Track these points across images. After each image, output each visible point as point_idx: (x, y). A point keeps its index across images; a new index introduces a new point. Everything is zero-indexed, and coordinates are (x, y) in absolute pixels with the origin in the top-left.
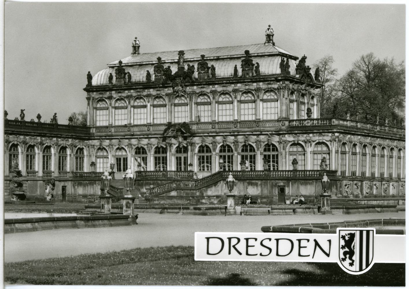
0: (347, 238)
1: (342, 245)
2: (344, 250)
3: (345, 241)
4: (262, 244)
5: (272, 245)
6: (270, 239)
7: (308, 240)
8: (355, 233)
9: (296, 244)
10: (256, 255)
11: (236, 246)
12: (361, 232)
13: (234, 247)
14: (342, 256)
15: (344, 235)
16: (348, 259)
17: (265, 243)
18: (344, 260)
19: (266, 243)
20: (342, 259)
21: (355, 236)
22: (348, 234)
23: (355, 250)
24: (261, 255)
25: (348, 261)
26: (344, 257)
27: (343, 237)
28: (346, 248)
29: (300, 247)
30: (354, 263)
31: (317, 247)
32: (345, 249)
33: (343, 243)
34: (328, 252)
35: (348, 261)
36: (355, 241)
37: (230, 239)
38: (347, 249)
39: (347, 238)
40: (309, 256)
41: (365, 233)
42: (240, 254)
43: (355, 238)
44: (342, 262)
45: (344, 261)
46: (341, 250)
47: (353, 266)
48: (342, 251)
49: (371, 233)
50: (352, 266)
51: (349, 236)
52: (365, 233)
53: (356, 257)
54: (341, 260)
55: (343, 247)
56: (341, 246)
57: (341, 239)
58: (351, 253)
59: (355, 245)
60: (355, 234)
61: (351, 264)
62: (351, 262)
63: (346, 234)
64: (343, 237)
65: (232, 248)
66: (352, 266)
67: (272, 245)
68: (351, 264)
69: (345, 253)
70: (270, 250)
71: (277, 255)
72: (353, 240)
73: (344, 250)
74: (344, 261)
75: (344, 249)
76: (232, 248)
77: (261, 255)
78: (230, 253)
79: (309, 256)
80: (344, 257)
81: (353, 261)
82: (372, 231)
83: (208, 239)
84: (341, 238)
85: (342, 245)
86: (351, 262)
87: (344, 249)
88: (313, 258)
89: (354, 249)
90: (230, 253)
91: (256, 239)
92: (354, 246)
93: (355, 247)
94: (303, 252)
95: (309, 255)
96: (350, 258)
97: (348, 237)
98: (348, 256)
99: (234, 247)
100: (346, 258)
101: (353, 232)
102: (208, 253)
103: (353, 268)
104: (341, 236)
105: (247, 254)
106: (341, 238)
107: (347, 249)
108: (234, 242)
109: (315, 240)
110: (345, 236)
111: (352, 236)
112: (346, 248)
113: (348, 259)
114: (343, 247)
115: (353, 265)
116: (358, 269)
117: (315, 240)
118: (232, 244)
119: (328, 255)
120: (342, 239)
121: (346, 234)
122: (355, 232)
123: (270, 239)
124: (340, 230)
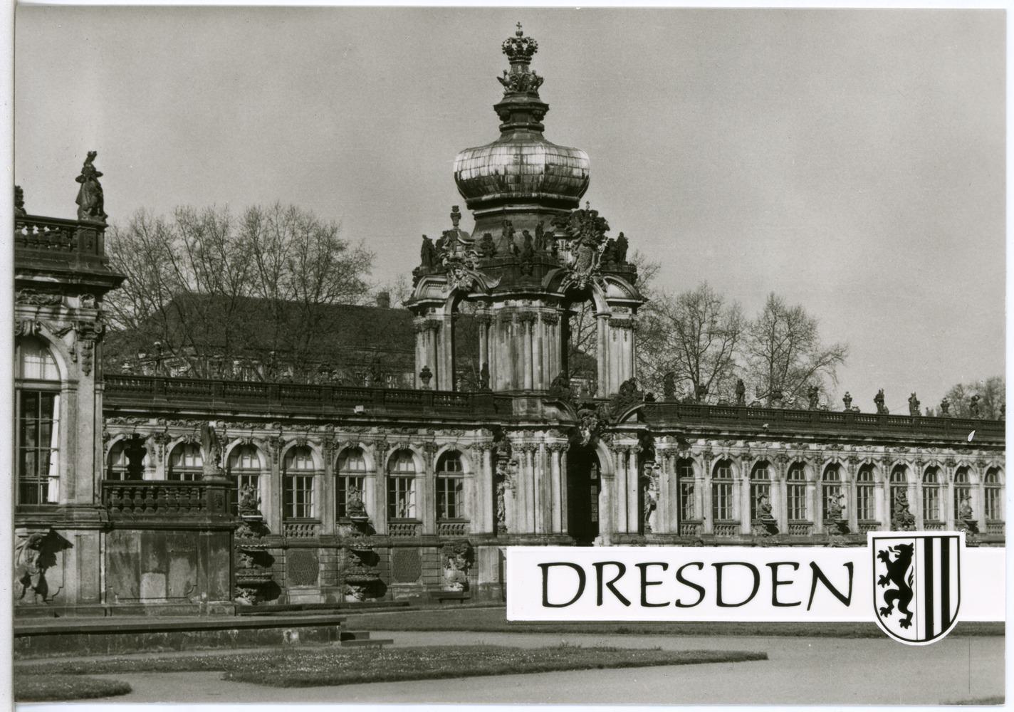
0: (893, 558)
1: (881, 576)
2: (887, 588)
3: (889, 565)
8: (912, 544)
12: (928, 542)
14: (882, 603)
15: (885, 549)
16: (896, 611)
18: (886, 612)
20: (882, 609)
21: (914, 552)
22: (896, 548)
23: (913, 588)
25: (897, 615)
26: (886, 606)
27: (884, 556)
28: (891, 581)
30: (913, 620)
32: (889, 584)
33: (882, 569)
35: (897, 615)
36: (913, 563)
38: (893, 586)
39: (893, 558)
41: (937, 545)
43: (913, 558)
44: (883, 618)
45: (886, 616)
46: (879, 587)
47: (909, 627)
48: (881, 591)
49: (953, 542)
50: (906, 628)
51: (898, 552)
52: (937, 545)
53: (917, 605)
54: (879, 612)
55: (884, 581)
56: (878, 579)
57: (879, 561)
58: (905, 595)
59: (914, 574)
60: (914, 547)
61: (905, 623)
62: (904, 616)
63: (890, 548)
64: (884, 556)
66: (906, 628)
68: (905, 623)
69: (889, 596)
72: (909, 562)
73: (887, 588)
74: (886, 616)
75: (886, 585)
80: (886, 606)
81: (910, 615)
82: (956, 539)
84: (879, 557)
85: (881, 576)
86: (904, 616)
87: (886, 585)
89: (911, 585)
92: (910, 577)
93: (914, 579)
96: (903, 608)
97: (896, 556)
98: (896, 602)
100: (891, 607)
101: (907, 542)
103: (909, 633)
104: (877, 553)
106: (879, 557)
107: (893, 586)
110: (887, 552)
111: (906, 552)
112: (891, 581)
113: (896, 611)
114: (884, 581)
115: (911, 624)
116: (922, 636)
120: (880, 559)
121: (890, 548)
122: (912, 541)
124: (874, 539)
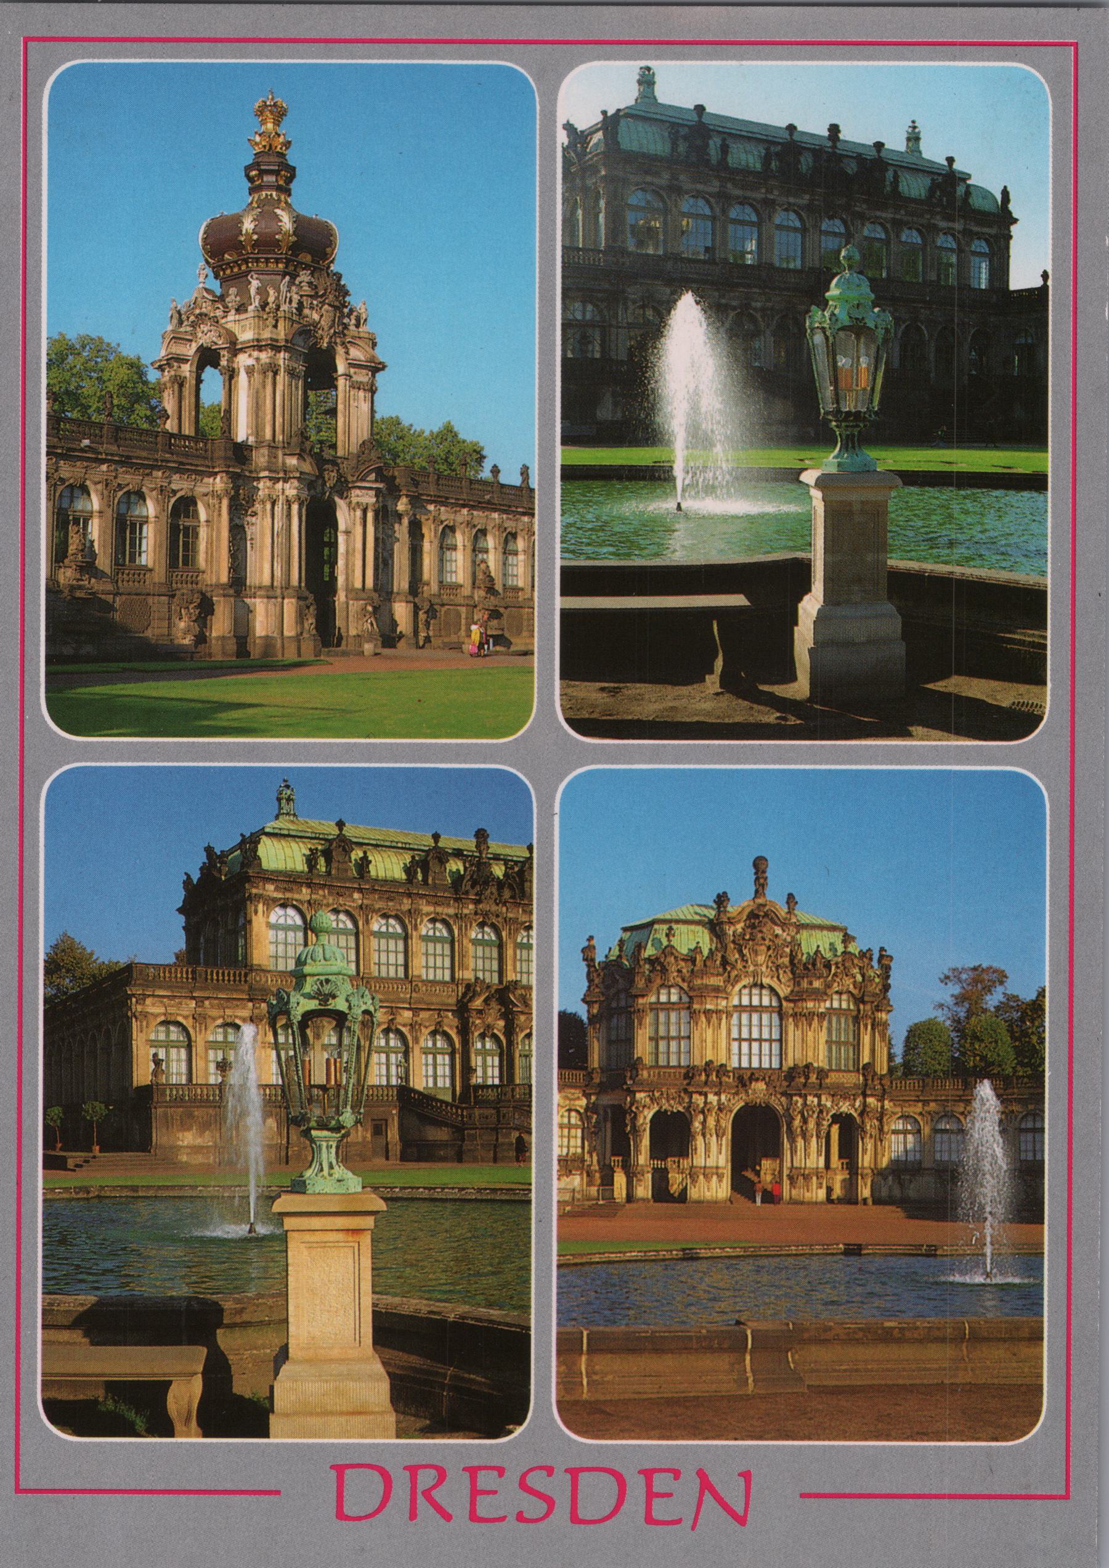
4: (523, 1485)
5: (558, 1487)
6: (550, 1470)
7: (677, 1474)
9: (636, 1488)
10: (502, 1519)
11: (434, 1493)
13: (427, 1494)
17: (534, 1481)
19: (536, 1480)
24: (520, 1517)
29: (651, 1495)
31: (708, 1496)
34: (740, 1510)
37: (413, 1470)
40: (678, 1521)
42: (448, 1517)
65: (421, 1500)
67: (558, 1487)
70: (550, 1502)
71: (575, 1519)
76: (421, 1500)
77: (520, 1517)
78: (413, 1515)
79: (678, 1521)
83: (340, 1470)
88: (693, 1528)
90: (413, 1515)
91: (501, 1471)
94: (660, 1509)
95: (675, 1518)
99: (427, 1494)
102: (341, 1515)
105: (474, 1517)
108: (426, 1478)
109: (701, 1474)
117: (701, 1474)
118: (421, 1488)
119: (742, 1520)
123: (550, 1470)
